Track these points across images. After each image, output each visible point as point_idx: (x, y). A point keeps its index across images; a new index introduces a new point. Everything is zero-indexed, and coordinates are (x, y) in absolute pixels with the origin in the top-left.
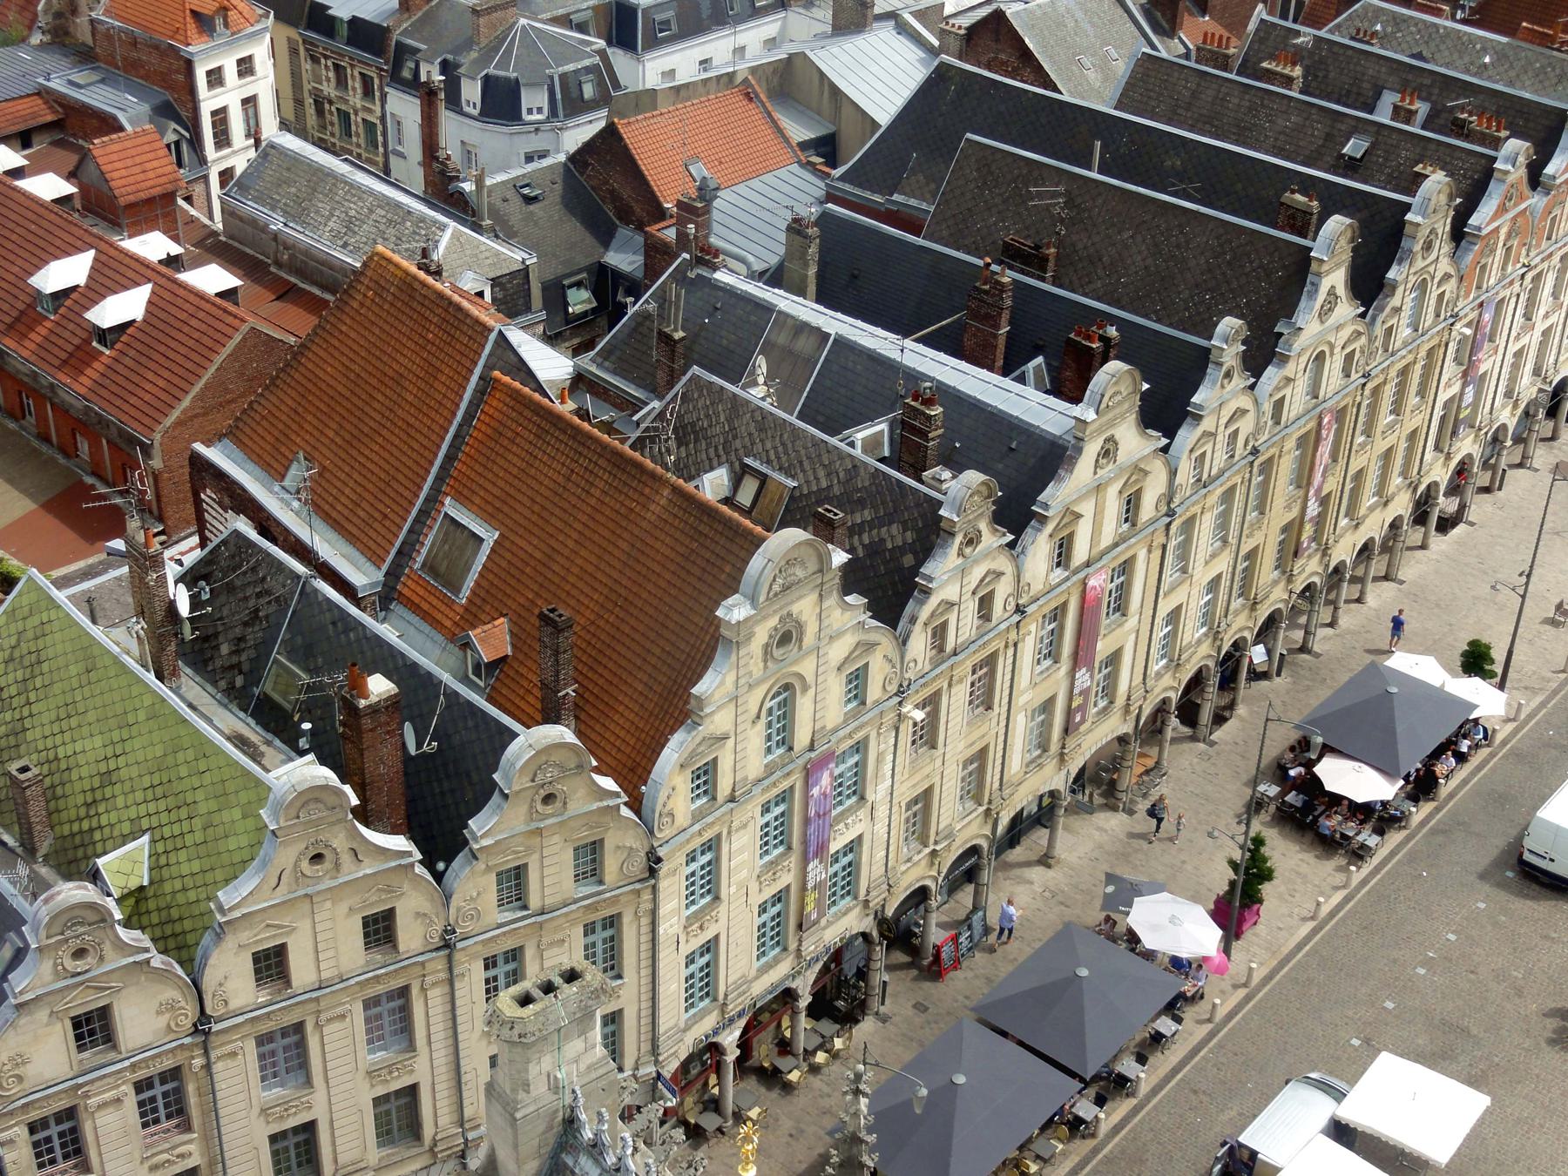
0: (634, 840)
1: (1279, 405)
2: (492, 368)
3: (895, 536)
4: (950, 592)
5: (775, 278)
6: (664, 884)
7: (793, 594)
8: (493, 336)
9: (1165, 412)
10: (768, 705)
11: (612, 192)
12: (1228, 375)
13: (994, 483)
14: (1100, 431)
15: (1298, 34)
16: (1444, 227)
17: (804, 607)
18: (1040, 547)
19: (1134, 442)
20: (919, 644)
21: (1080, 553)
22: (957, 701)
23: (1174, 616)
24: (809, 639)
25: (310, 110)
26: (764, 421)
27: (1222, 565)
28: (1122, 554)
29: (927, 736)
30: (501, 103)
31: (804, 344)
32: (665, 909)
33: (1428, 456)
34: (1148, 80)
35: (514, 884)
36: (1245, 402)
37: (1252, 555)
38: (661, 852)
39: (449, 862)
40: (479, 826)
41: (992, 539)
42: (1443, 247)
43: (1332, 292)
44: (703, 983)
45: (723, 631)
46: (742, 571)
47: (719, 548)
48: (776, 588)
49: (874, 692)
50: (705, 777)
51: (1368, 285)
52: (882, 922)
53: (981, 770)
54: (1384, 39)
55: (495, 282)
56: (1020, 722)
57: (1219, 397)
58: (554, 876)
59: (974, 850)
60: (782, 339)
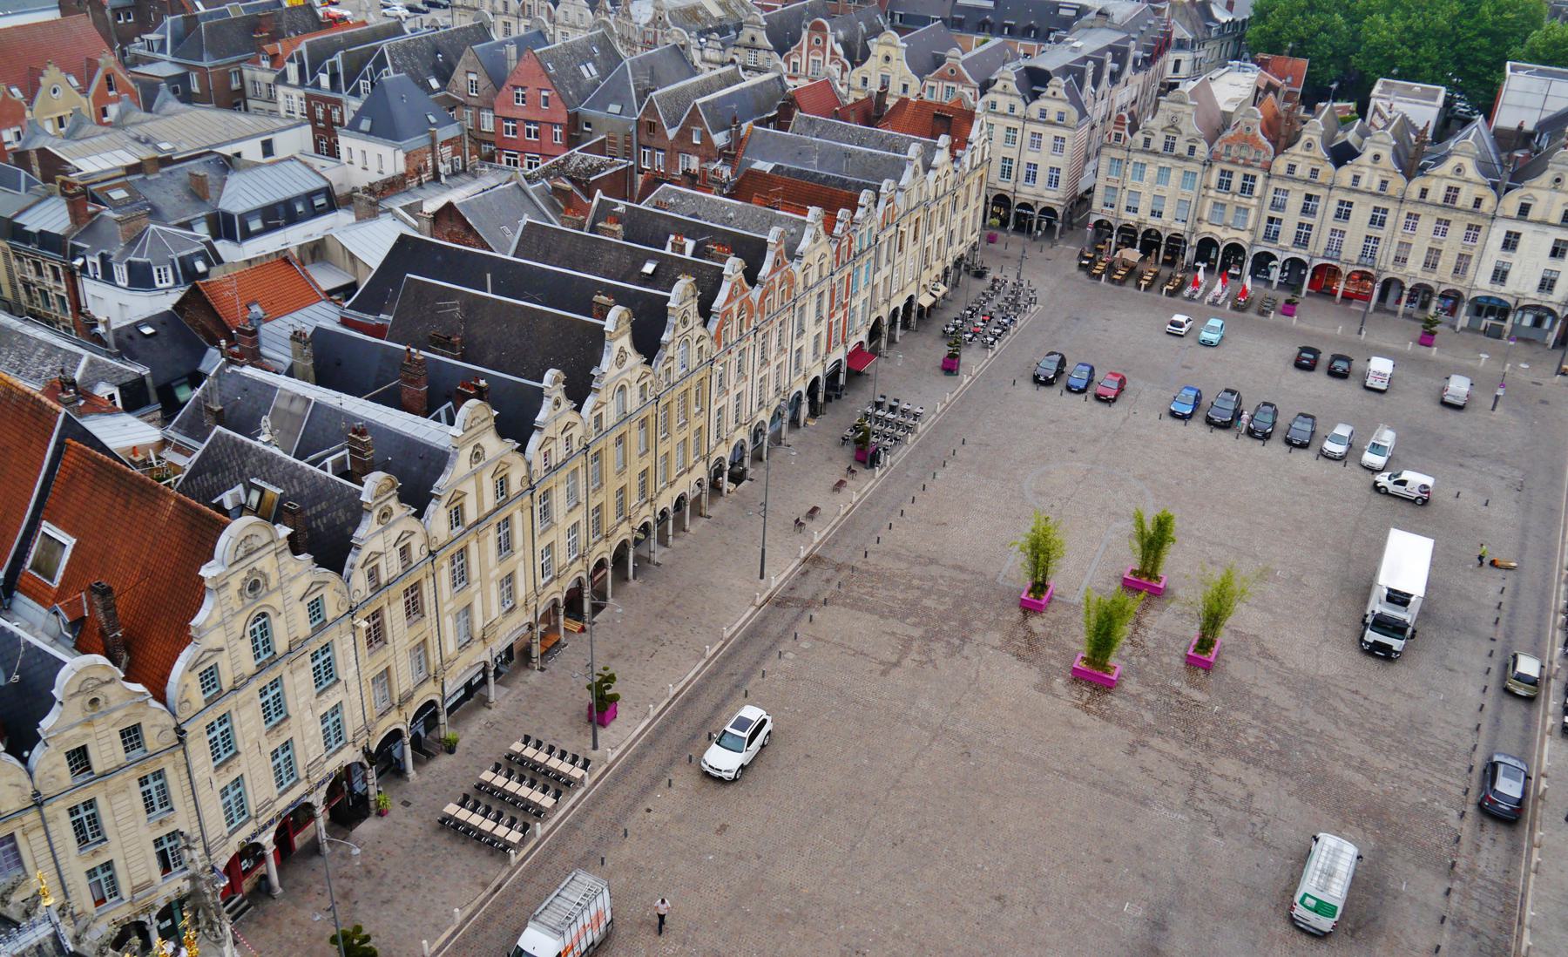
0: (166, 719)
1: (599, 418)
2: (66, 436)
3: (341, 516)
4: (376, 544)
5: (290, 373)
6: (191, 747)
7: (255, 556)
8: (61, 417)
9: (516, 424)
10: (249, 629)
11: (202, 326)
12: (557, 403)
13: (394, 478)
14: (468, 441)
15: (616, 205)
16: (693, 306)
17: (265, 562)
18: (438, 514)
19: (493, 446)
20: (360, 581)
21: (471, 515)
22: (395, 615)
23: (550, 547)
24: (273, 583)
25: (22, 291)
26: (269, 460)
27: (579, 515)
28: (503, 514)
29: (377, 635)
30: (141, 278)
31: (297, 407)
32: (196, 763)
33: (712, 443)
34: (534, 240)
35: (79, 758)
36: (573, 417)
37: (598, 508)
38: (184, 727)
39: (31, 750)
40: (46, 724)
41: (400, 510)
42: (695, 320)
43: (622, 350)
44: (236, 808)
45: (208, 584)
46: (215, 544)
47: (201, 535)
48: (240, 554)
49: (330, 612)
50: (209, 678)
51: (648, 342)
52: (367, 752)
53: (426, 652)
54: (672, 207)
55: (122, 388)
56: (449, 623)
57: (552, 413)
58: (106, 752)
59: (432, 703)
60: (283, 405)
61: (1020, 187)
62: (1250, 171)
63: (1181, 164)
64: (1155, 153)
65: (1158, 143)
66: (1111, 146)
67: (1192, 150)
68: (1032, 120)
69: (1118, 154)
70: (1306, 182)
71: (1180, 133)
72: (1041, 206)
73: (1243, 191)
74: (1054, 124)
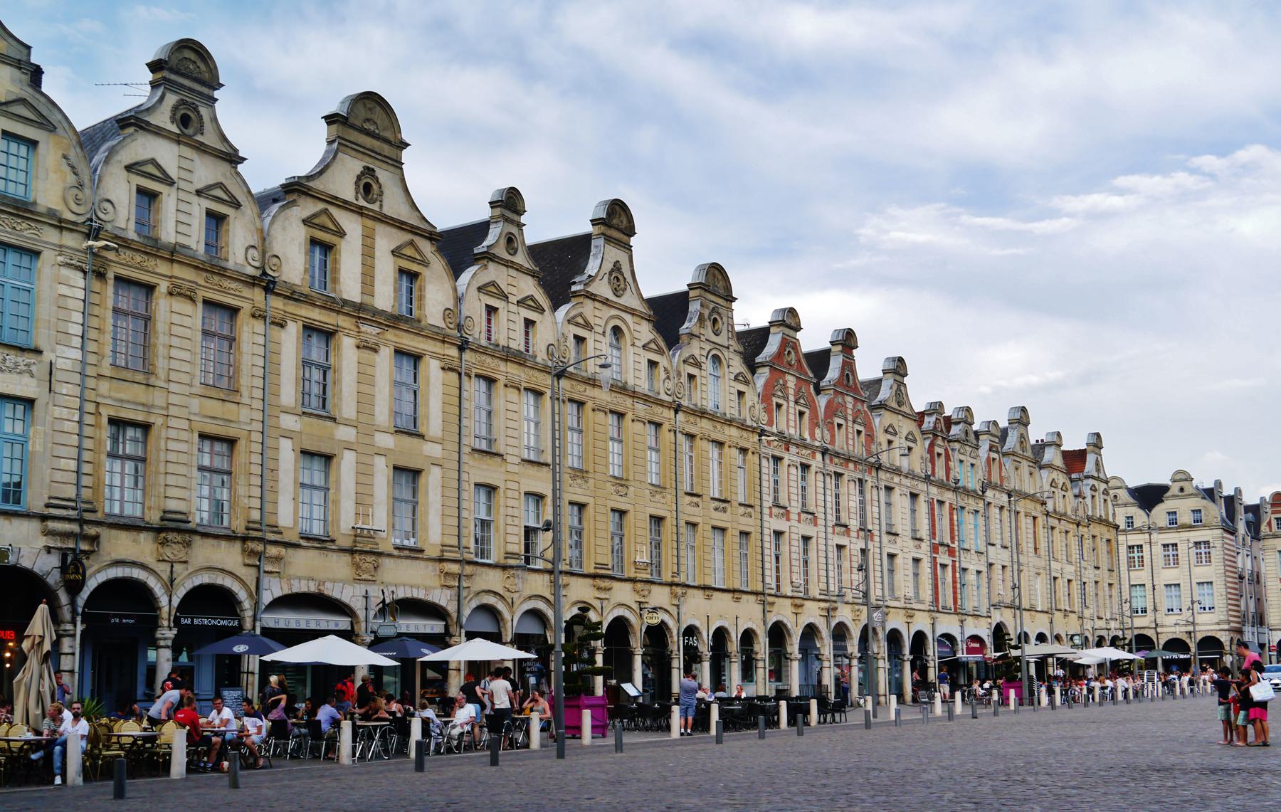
68: (1161, 529)
72: (1199, 636)
74: (1191, 527)
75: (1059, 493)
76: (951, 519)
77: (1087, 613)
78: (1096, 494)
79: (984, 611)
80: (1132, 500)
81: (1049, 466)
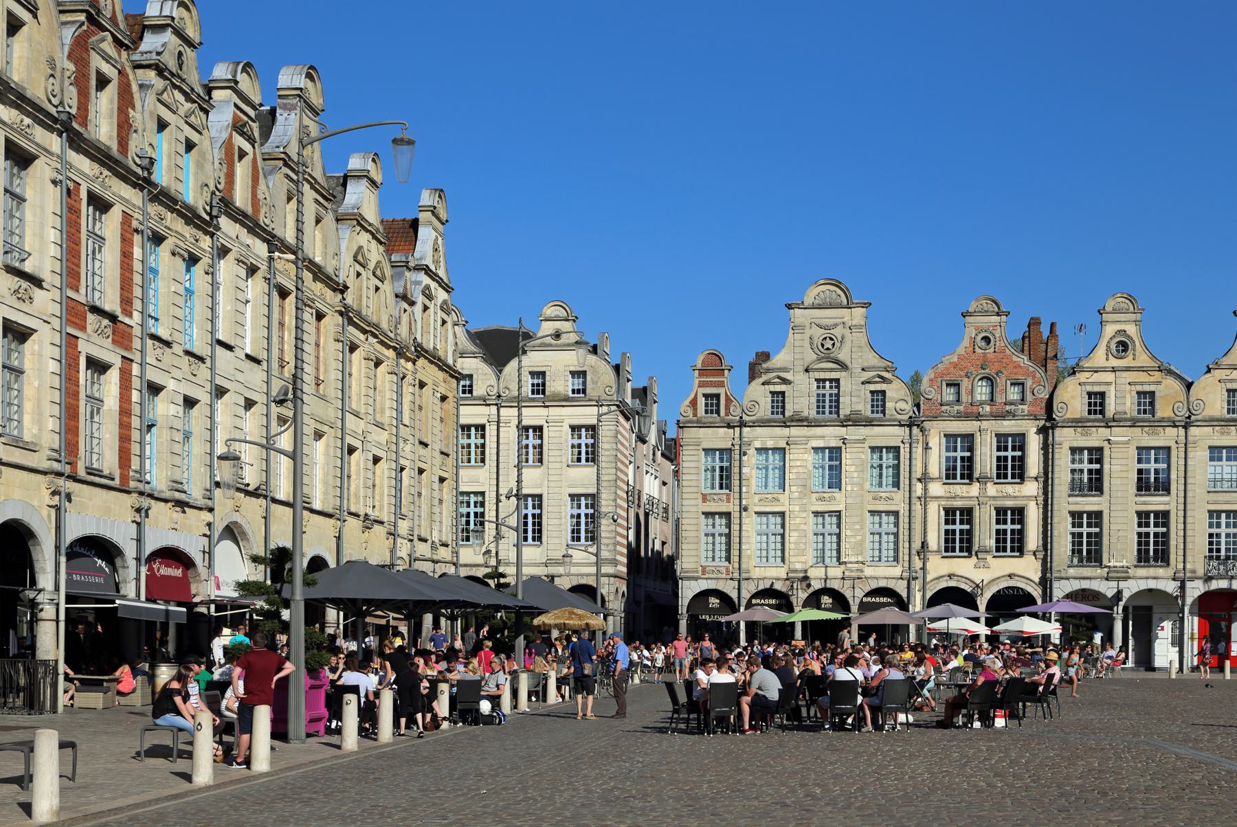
61: (507, 550)
62: (1008, 426)
63: (862, 432)
64: (800, 421)
65: (802, 398)
66: (701, 425)
67: (879, 398)
68: (519, 402)
69: (721, 437)
70: (1134, 423)
71: (843, 367)
73: (1001, 474)
75: (369, 281)
76: (126, 255)
77: (403, 527)
78: (432, 307)
79: (196, 493)
80: (472, 348)
81: (360, 222)
